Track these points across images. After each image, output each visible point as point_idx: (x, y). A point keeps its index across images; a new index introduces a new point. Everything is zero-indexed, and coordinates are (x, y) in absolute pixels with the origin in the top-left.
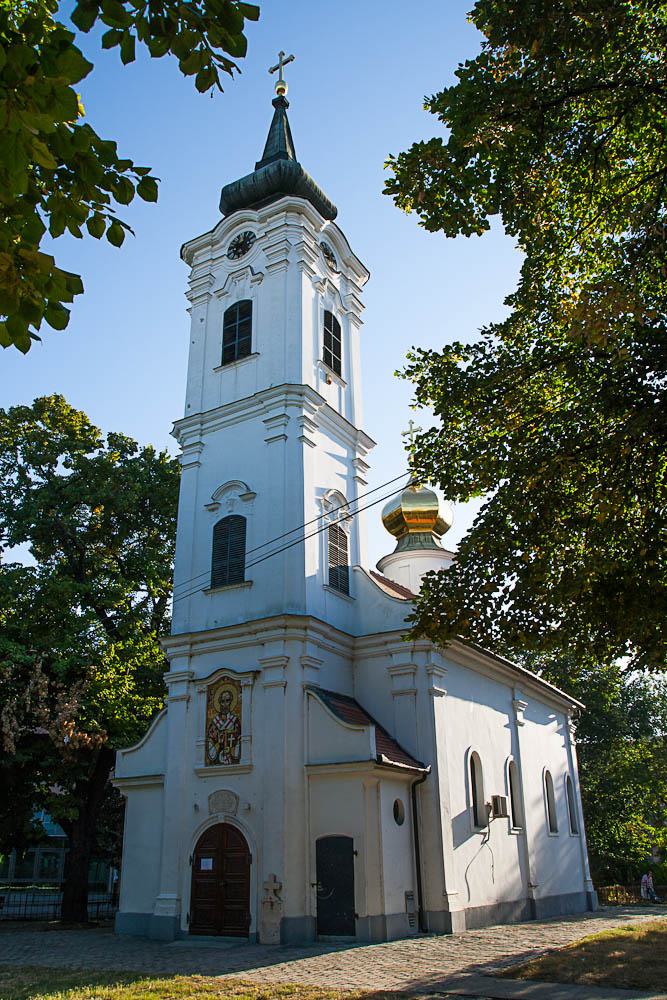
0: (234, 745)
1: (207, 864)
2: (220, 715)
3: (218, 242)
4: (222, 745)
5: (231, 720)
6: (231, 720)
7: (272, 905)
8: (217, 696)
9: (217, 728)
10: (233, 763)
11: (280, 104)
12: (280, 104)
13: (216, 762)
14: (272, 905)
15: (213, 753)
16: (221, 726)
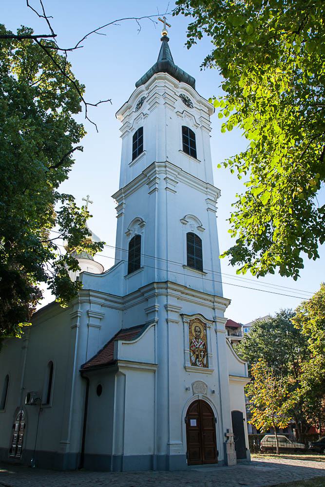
0: (204, 357)
1: (193, 423)
2: (196, 338)
3: (178, 88)
4: (197, 355)
5: (201, 343)
6: (201, 343)
7: (231, 445)
8: (193, 328)
9: (194, 345)
10: (203, 367)
11: (165, 39)
12: (165, 39)
13: (194, 364)
14: (231, 445)
15: (193, 359)
16: (197, 345)
